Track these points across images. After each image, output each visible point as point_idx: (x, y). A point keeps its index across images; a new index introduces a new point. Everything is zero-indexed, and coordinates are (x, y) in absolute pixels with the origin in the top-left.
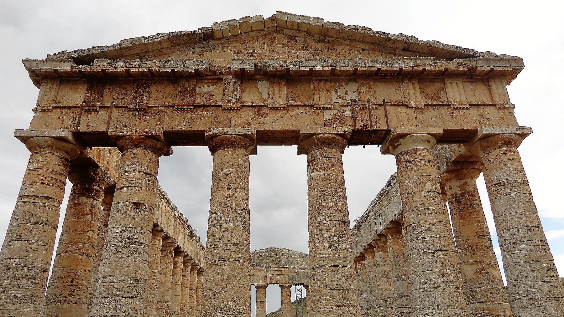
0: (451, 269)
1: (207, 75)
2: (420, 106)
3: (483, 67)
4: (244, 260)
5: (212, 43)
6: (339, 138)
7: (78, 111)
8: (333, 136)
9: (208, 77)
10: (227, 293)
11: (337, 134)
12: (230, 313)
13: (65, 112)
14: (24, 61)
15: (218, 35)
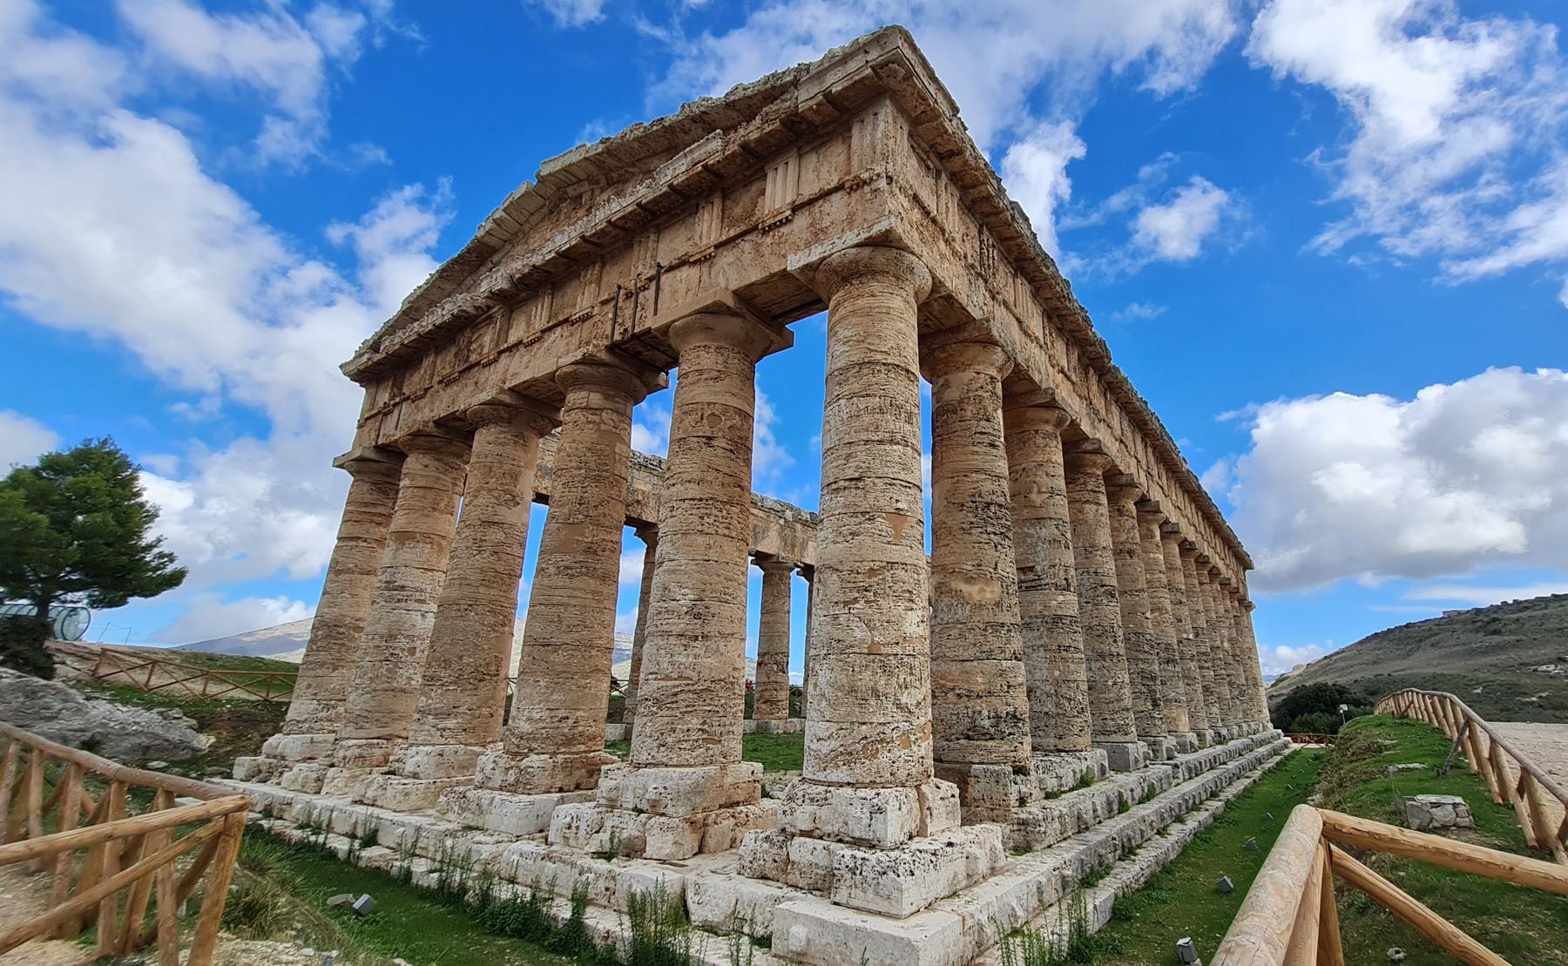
1: (477, 317)
2: (708, 251)
3: (806, 97)
5: (495, 258)
6: (582, 368)
7: (380, 416)
8: (571, 368)
9: (479, 320)
11: (576, 363)
13: (373, 420)
14: (341, 367)
15: (493, 241)
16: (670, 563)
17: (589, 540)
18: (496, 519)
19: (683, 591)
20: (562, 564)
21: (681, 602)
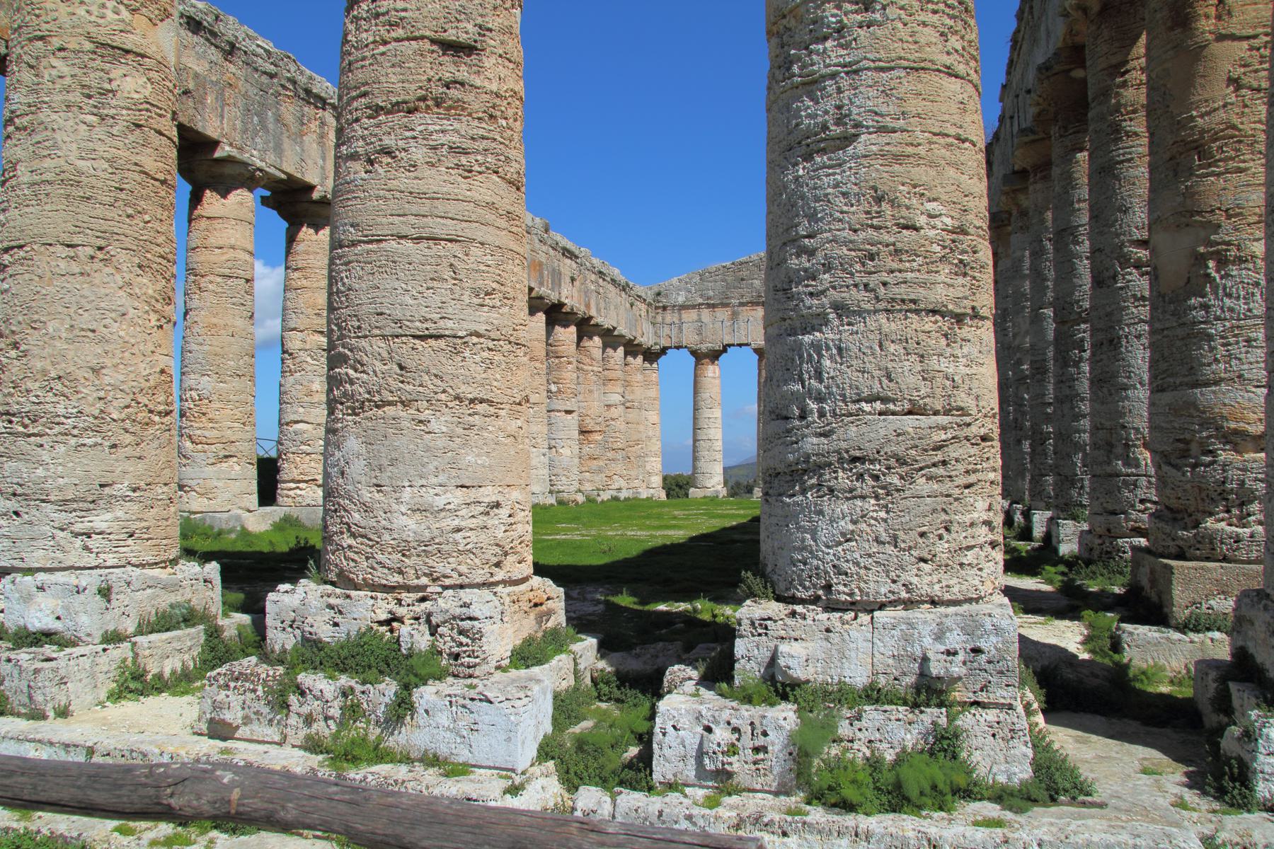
0: (922, 220)
4: (101, 243)
10: (25, 360)
12: (36, 431)
16: (884, 138)
17: (495, 89)
18: (129, 41)
19: (930, 206)
20: (443, 139)
21: (932, 233)
